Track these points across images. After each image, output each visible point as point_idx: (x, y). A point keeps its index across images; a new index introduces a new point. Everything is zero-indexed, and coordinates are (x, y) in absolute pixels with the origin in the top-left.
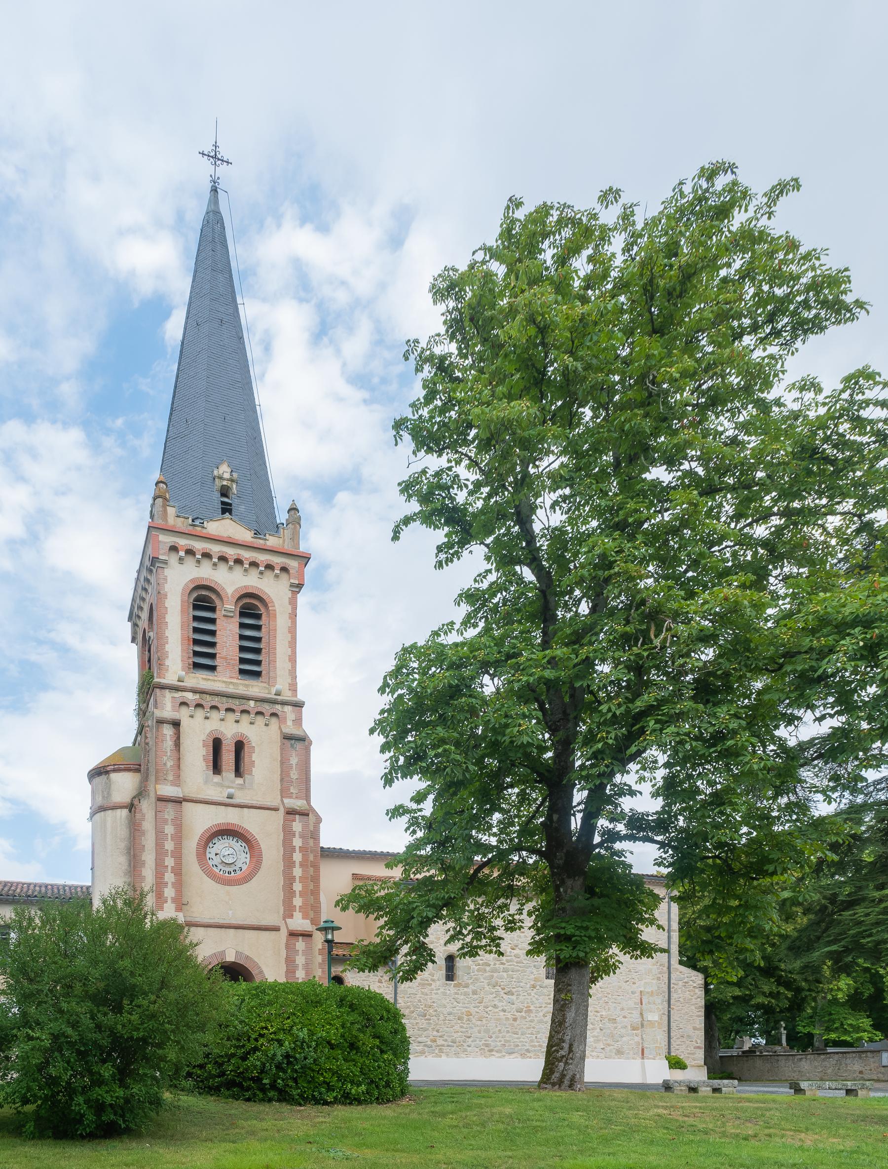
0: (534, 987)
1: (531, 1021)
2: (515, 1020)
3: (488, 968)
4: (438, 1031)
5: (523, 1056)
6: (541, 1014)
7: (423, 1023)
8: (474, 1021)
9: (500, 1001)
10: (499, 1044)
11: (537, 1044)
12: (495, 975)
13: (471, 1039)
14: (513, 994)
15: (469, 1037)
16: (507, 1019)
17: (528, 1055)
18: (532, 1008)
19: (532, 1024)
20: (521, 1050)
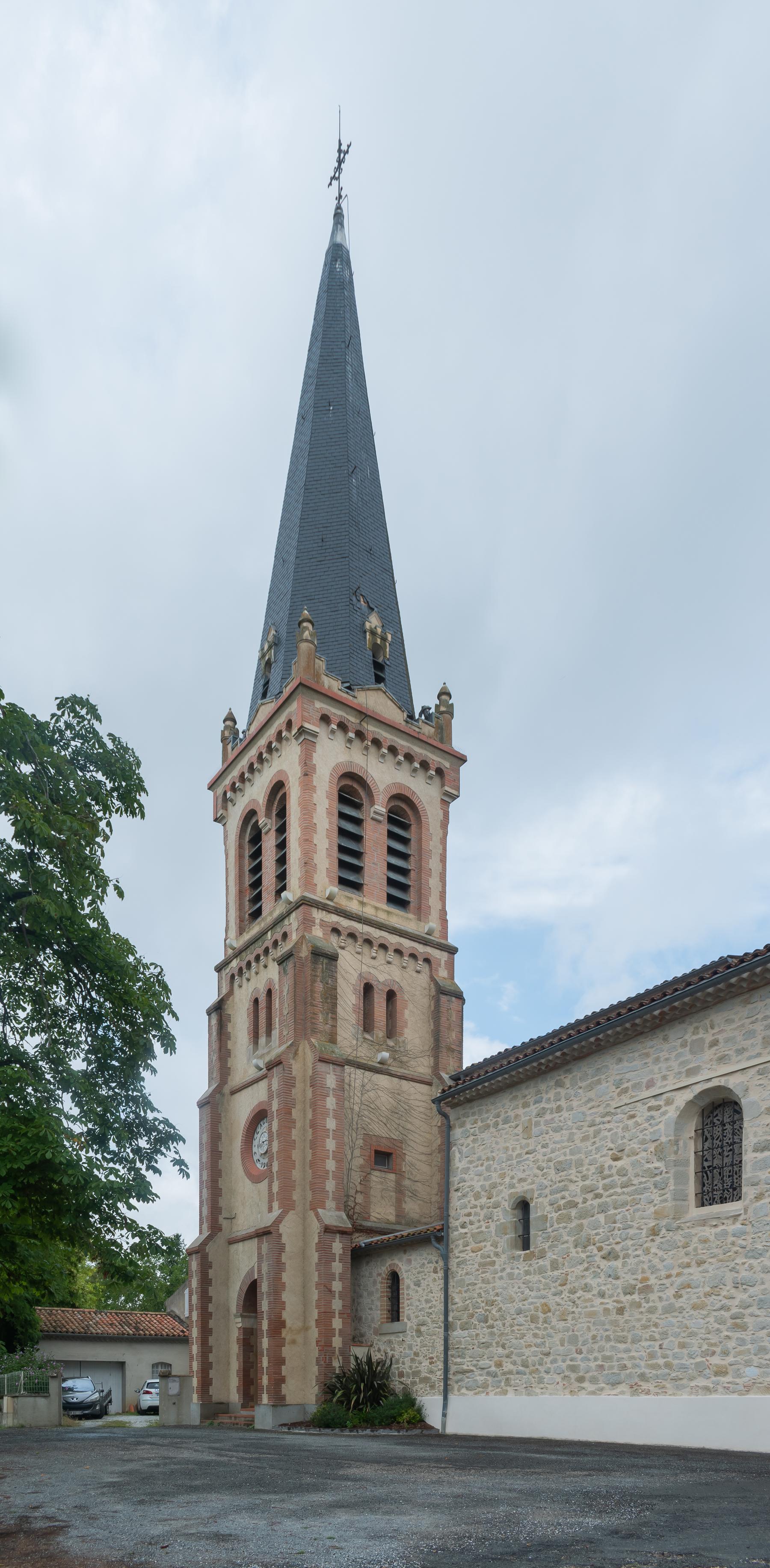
0: (654, 1232)
1: (652, 1310)
2: (621, 1311)
3: (573, 1212)
6: (671, 1292)
8: (554, 1321)
9: (596, 1275)
11: (661, 1361)
12: (585, 1222)
14: (616, 1258)
16: (607, 1311)
17: (645, 1386)
18: (652, 1281)
19: (654, 1317)
20: (630, 1376)
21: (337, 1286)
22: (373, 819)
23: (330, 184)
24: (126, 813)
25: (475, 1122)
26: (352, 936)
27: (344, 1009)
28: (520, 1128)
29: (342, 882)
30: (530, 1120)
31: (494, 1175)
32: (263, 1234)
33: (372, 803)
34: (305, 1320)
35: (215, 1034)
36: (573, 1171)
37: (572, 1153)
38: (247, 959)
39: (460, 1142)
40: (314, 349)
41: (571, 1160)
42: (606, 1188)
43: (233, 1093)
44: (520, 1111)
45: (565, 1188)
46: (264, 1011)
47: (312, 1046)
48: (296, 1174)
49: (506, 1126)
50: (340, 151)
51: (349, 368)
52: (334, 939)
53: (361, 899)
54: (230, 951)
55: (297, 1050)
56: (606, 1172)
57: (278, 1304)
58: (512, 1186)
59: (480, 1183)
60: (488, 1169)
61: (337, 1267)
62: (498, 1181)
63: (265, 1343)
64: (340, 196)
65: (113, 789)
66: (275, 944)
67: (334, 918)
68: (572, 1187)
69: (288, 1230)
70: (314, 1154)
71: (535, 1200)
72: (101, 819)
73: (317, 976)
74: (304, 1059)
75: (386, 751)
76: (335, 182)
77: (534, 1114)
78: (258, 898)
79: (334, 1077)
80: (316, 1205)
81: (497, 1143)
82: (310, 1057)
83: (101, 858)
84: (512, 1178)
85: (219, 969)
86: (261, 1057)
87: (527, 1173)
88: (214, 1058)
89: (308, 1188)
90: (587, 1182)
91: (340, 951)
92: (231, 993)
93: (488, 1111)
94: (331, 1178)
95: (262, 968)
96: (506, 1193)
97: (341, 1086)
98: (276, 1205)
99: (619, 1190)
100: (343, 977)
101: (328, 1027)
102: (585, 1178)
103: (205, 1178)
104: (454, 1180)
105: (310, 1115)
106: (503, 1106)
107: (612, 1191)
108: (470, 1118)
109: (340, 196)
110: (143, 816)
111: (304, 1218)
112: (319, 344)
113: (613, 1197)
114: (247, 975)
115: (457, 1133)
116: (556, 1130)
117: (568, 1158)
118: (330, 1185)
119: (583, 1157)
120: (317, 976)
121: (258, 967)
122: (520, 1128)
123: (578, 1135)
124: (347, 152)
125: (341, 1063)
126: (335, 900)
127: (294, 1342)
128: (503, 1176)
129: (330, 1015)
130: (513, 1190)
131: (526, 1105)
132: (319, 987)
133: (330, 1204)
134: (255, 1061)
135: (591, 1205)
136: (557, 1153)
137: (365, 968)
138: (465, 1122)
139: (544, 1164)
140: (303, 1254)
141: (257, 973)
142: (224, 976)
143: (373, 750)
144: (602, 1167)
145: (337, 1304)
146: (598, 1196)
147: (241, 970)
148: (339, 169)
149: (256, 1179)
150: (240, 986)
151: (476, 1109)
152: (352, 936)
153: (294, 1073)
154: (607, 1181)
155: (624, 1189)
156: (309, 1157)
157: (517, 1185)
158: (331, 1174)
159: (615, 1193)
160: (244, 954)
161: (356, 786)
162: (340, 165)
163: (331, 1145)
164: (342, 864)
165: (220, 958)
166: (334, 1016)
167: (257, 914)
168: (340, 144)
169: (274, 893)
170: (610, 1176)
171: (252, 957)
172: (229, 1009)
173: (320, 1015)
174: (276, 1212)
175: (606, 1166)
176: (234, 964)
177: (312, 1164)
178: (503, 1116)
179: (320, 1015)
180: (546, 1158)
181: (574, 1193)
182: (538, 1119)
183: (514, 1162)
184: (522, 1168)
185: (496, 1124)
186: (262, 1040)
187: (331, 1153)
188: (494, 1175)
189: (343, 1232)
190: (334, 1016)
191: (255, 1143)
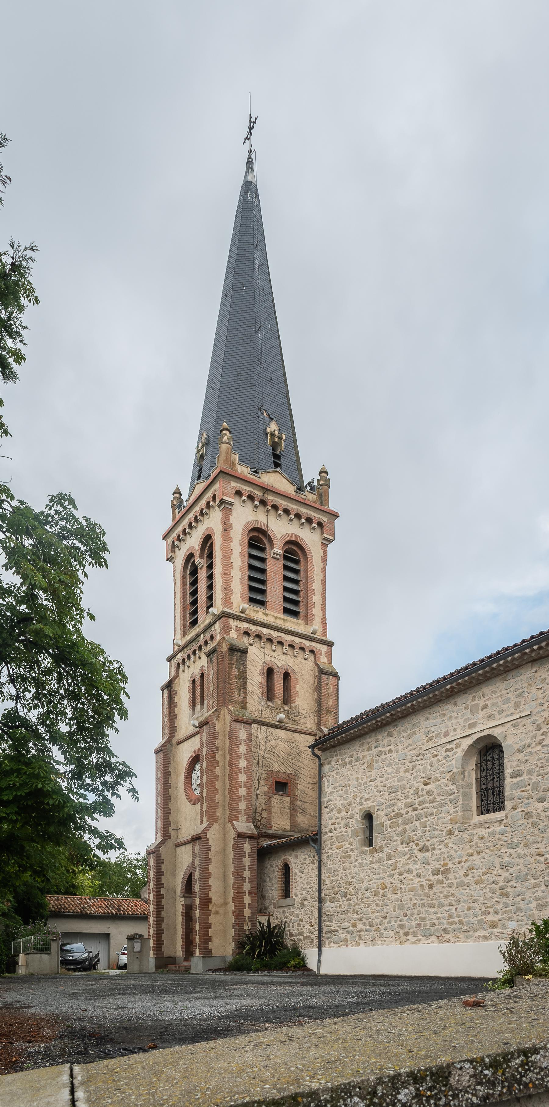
0: (451, 833)
1: (450, 886)
2: (431, 886)
3: (400, 820)
4: (357, 913)
5: (441, 939)
6: (462, 873)
7: (344, 903)
8: (389, 895)
9: (415, 862)
10: (414, 923)
11: (456, 920)
12: (407, 827)
13: (387, 920)
14: (427, 850)
15: (385, 917)
16: (422, 886)
17: (447, 937)
18: (450, 865)
19: (451, 890)
20: (437, 930)
22: (273, 557)
23: (245, 142)
24: (96, 565)
25: (338, 761)
26: (258, 636)
27: (253, 686)
28: (366, 765)
29: (252, 600)
30: (372, 759)
31: (350, 796)
32: (196, 839)
33: (272, 547)
34: (225, 898)
35: (166, 703)
36: (400, 793)
37: (398, 781)
38: (188, 653)
39: (328, 774)
40: (233, 250)
41: (398, 785)
42: (420, 804)
43: (179, 743)
44: (366, 753)
45: (394, 805)
46: (199, 688)
47: (230, 711)
48: (219, 798)
49: (357, 763)
50: (250, 121)
51: (256, 261)
52: (245, 640)
53: (264, 611)
54: (177, 648)
55: (220, 714)
56: (420, 793)
57: (206, 887)
58: (361, 804)
59: (341, 802)
60: (346, 793)
62: (353, 800)
63: (197, 913)
64: (251, 151)
65: (86, 551)
66: (206, 643)
67: (245, 625)
68: (399, 803)
69: (213, 836)
70: (231, 784)
71: (376, 813)
72: (78, 570)
73: (233, 664)
74: (224, 720)
75: (282, 513)
76: (247, 141)
77: (374, 755)
78: (195, 612)
79: (245, 732)
80: (232, 819)
81: (351, 775)
82: (228, 719)
83: (81, 594)
84: (361, 798)
85: (170, 659)
87: (370, 795)
88: (166, 720)
89: (227, 807)
90: (408, 800)
91: (249, 647)
92: (177, 675)
93: (345, 753)
94: (243, 800)
95: (197, 659)
96: (357, 808)
98: (205, 819)
99: (428, 805)
100: (252, 664)
101: (241, 698)
102: (407, 797)
103: (159, 802)
104: (324, 800)
105: (228, 758)
106: (355, 749)
107: (424, 806)
108: (335, 758)
109: (251, 151)
110: (107, 567)
111: (224, 828)
112: (236, 247)
113: (425, 810)
114: (188, 664)
115: (326, 768)
116: (389, 765)
117: (396, 784)
118: (242, 805)
119: (405, 783)
120: (233, 664)
121: (195, 658)
122: (366, 765)
123: (402, 769)
124: (255, 122)
125: (249, 723)
126: (246, 613)
127: (217, 913)
128: (355, 797)
129: (242, 690)
130: (361, 807)
131: (369, 749)
132: (235, 671)
133: (242, 818)
134: (192, 722)
135: (411, 815)
136: (389, 781)
137: (267, 658)
138: (331, 761)
139: (381, 789)
140: (224, 852)
141: (194, 662)
142: (173, 664)
143: (272, 512)
144: (417, 789)
146: (415, 809)
147: (183, 660)
148: (250, 133)
149: (193, 802)
150: (184, 671)
151: (338, 752)
152: (258, 636)
153: (217, 729)
154: (421, 799)
155: (432, 804)
156: (228, 786)
157: (364, 803)
158: (243, 797)
159: (426, 807)
160: (185, 649)
161: (261, 536)
162: (250, 130)
163: (242, 778)
164: (251, 589)
165: (171, 652)
166: (245, 691)
167: (194, 623)
168: (251, 117)
169: (205, 609)
170: (423, 795)
171: (190, 652)
172: (176, 687)
173: (235, 690)
174: (205, 824)
175: (420, 789)
176: (180, 656)
177: (230, 791)
178: (355, 756)
179: (235, 690)
180: (382, 784)
181: (400, 808)
182: (378, 758)
183: (363, 787)
184: (367, 791)
185: (351, 762)
186: (198, 707)
187: (243, 783)
188: (350, 796)
190: (245, 691)
191: (194, 777)
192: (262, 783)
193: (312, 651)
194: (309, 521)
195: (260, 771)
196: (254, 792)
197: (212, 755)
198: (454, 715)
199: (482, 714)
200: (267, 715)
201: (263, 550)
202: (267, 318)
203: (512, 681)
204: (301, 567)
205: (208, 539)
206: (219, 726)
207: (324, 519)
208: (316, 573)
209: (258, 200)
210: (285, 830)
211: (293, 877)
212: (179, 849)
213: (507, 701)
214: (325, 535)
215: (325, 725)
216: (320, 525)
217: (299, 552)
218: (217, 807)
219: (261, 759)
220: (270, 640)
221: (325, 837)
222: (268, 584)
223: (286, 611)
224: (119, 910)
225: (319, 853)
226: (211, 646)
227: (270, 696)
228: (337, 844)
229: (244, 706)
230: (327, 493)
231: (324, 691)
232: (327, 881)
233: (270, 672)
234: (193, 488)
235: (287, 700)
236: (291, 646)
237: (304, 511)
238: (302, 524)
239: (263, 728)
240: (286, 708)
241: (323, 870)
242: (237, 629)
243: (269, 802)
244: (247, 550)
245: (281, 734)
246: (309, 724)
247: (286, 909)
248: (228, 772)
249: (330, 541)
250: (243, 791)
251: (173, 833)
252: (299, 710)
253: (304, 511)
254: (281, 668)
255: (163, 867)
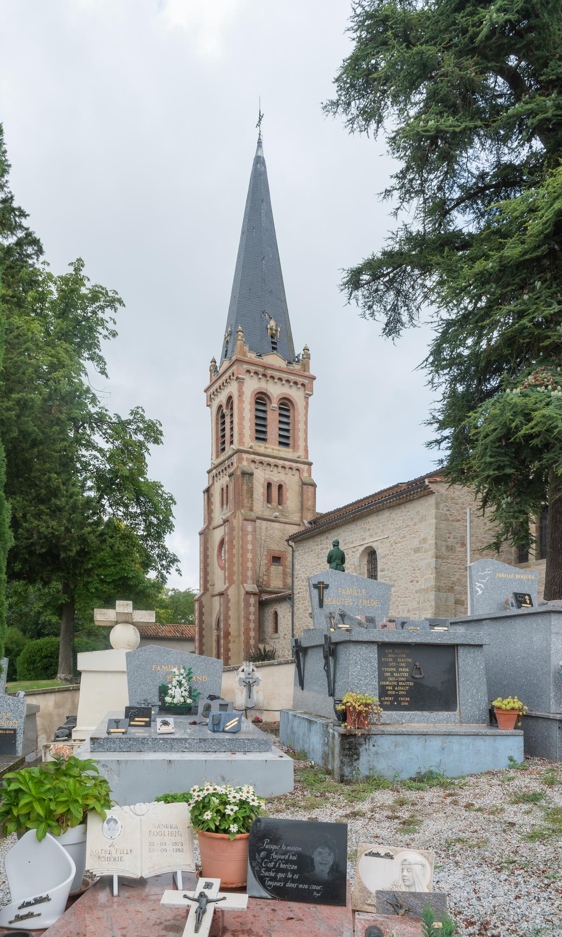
21: (252, 617)
26: (261, 463)
32: (221, 594)
33: (271, 403)
34: (239, 633)
48: (235, 568)
52: (253, 465)
57: (227, 625)
61: (252, 609)
63: (222, 641)
67: (253, 456)
69: (232, 593)
80: (244, 581)
86: (224, 514)
97: (254, 530)
98: (227, 581)
105: (241, 543)
111: (239, 588)
118: (250, 573)
127: (234, 642)
132: (245, 487)
133: (250, 581)
137: (267, 476)
140: (238, 603)
145: (252, 625)
152: (261, 463)
174: (227, 585)
177: (242, 564)
189: (254, 594)
192: (264, 558)
193: (298, 470)
194: (296, 383)
195: (262, 550)
196: (258, 564)
197: (231, 541)
198: (356, 531)
199: (368, 533)
200: (267, 514)
201: (265, 405)
202: (269, 249)
203: (381, 517)
204: (290, 414)
205: (230, 398)
206: (235, 522)
207: (306, 381)
208: (300, 417)
209: (265, 167)
210: (279, 588)
211: (279, 620)
212: (214, 598)
213: (378, 528)
214: (307, 392)
215: (306, 519)
216: (303, 385)
217: (289, 404)
218: (234, 574)
219: (263, 542)
220: (269, 464)
221: (295, 597)
222: (268, 427)
223: (281, 443)
224: (182, 634)
225: (293, 606)
226: (231, 470)
227: (269, 500)
228: (302, 602)
229: (251, 510)
230: (308, 363)
231: (305, 496)
232: (296, 624)
233: (269, 485)
234: (222, 363)
235: (280, 503)
236: (283, 467)
237: (292, 378)
238: (291, 386)
239: (264, 522)
240: (280, 507)
241: (295, 617)
242: (247, 459)
243: (268, 570)
244: (254, 406)
245: (276, 525)
246: (296, 518)
247: (276, 640)
248: (241, 552)
249: (310, 395)
250: (250, 565)
251: (210, 588)
252: (289, 509)
253: (292, 378)
254: (277, 482)
255: (204, 610)
